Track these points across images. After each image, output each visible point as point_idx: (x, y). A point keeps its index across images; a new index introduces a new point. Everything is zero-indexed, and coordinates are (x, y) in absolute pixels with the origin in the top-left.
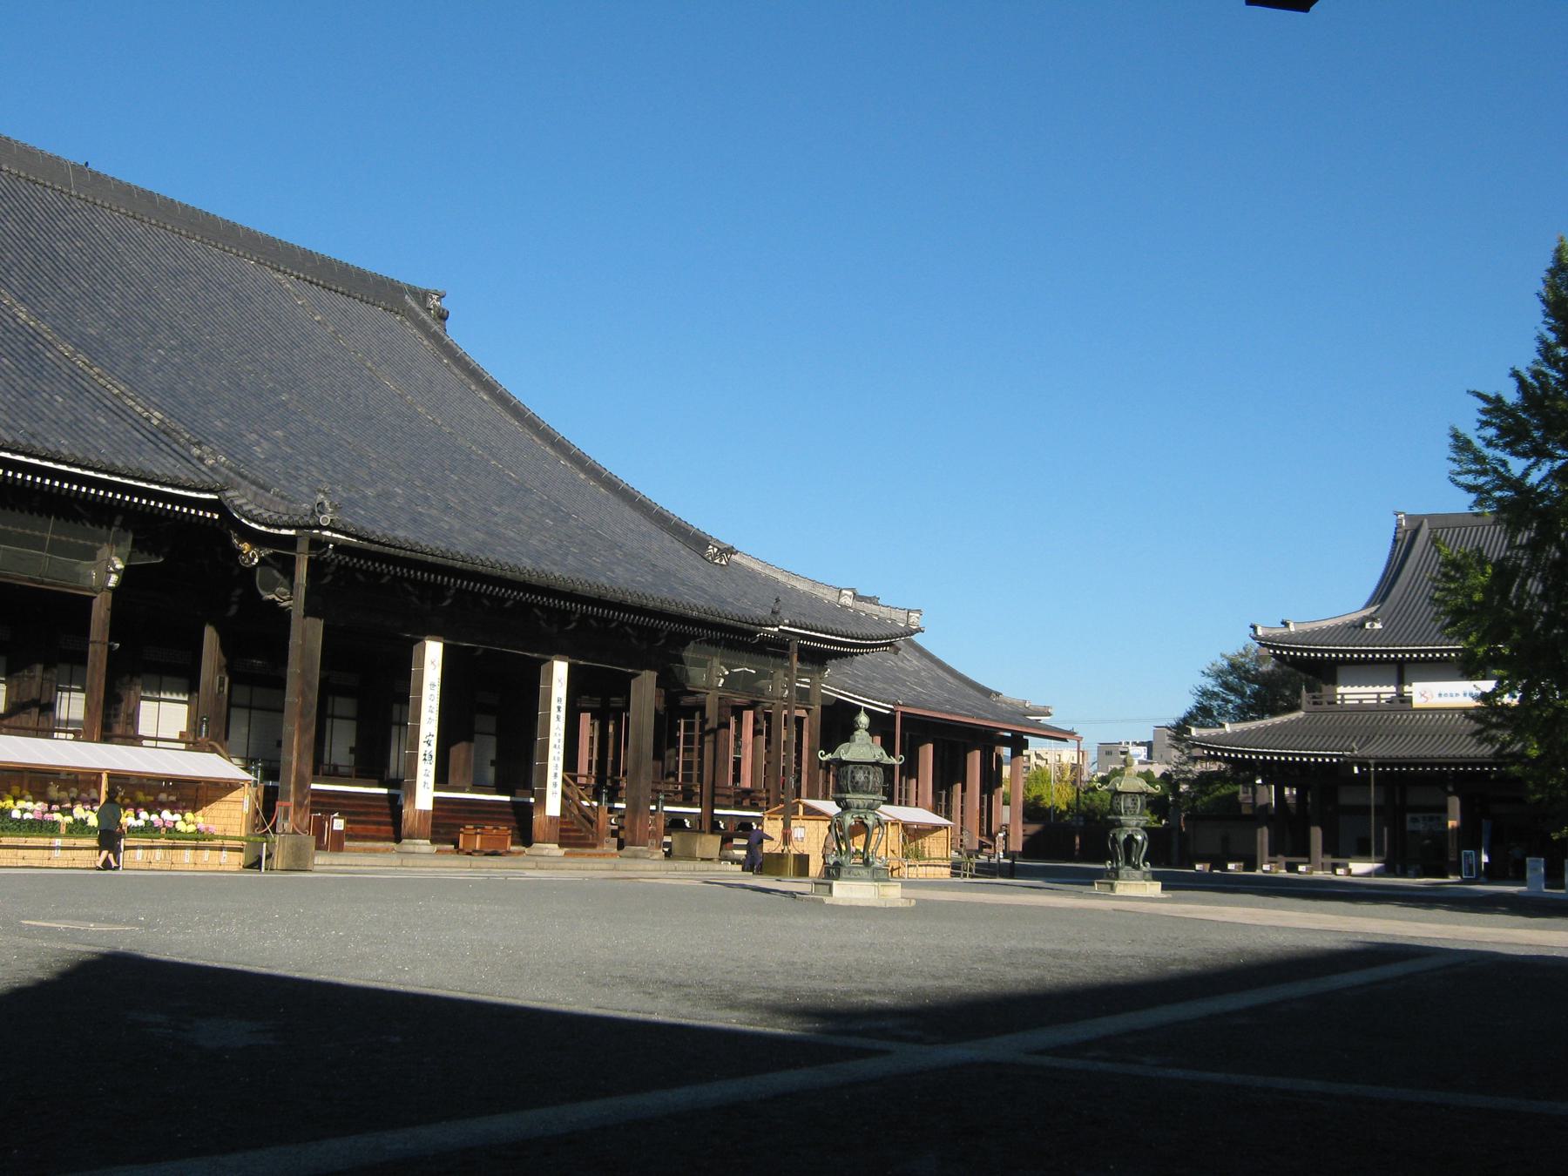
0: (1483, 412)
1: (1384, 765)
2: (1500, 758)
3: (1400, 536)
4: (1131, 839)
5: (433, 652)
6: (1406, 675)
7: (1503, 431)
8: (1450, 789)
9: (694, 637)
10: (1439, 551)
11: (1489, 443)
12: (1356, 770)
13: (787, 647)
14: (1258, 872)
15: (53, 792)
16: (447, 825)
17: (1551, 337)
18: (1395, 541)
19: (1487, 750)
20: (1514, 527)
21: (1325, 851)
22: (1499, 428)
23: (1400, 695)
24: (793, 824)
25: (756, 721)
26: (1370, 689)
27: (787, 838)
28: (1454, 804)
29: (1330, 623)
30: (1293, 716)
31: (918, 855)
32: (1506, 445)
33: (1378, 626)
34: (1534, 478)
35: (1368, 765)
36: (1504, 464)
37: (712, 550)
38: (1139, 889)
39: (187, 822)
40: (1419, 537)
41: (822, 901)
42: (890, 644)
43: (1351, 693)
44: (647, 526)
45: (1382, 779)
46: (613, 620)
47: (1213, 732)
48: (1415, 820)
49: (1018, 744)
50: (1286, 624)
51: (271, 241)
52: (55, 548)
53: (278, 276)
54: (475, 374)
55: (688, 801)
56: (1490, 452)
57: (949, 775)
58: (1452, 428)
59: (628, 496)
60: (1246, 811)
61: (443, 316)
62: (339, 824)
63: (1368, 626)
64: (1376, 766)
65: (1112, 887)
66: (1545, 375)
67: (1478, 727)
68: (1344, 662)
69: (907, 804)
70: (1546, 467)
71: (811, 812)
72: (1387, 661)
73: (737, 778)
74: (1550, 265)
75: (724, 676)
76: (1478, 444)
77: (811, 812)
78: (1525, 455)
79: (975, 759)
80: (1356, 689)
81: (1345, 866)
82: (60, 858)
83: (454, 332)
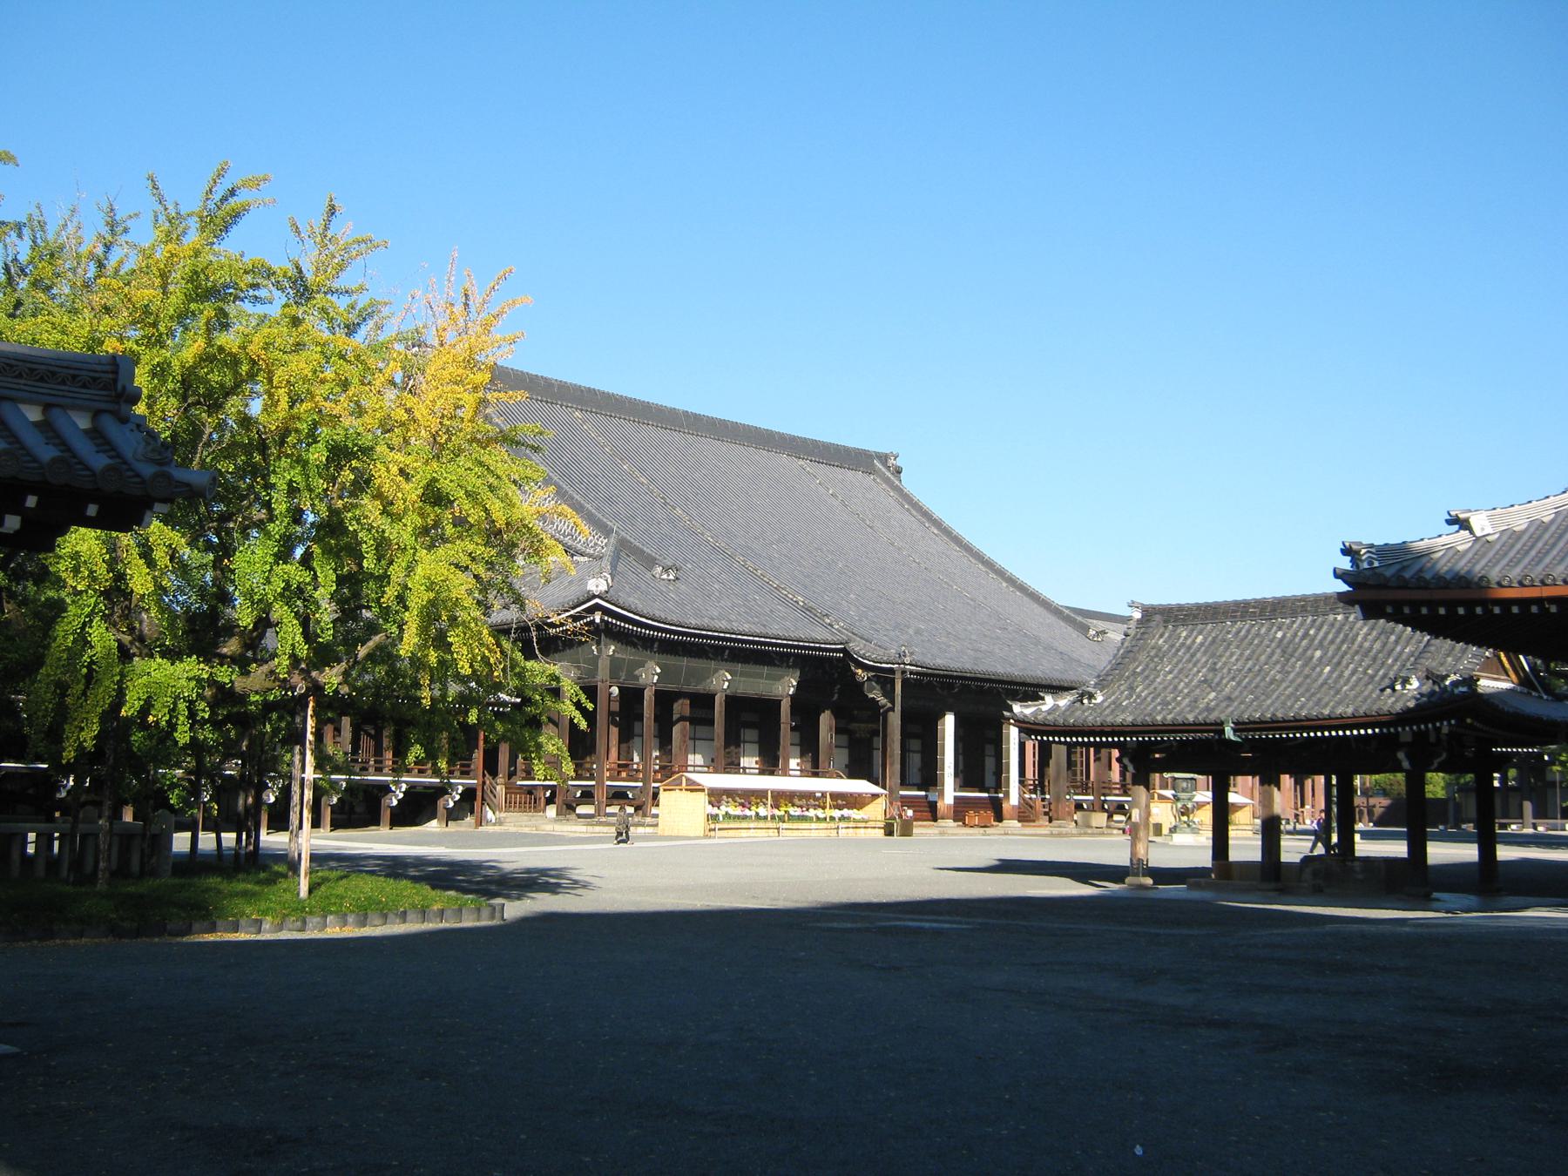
5: (949, 721)
15: (796, 801)
16: (961, 811)
37: (1092, 632)
39: (854, 814)
44: (1051, 619)
51: (793, 439)
52: (769, 677)
53: (801, 462)
54: (927, 515)
61: (898, 471)
62: (910, 813)
71: (1162, 797)
77: (1162, 797)
82: (814, 834)
83: (908, 482)
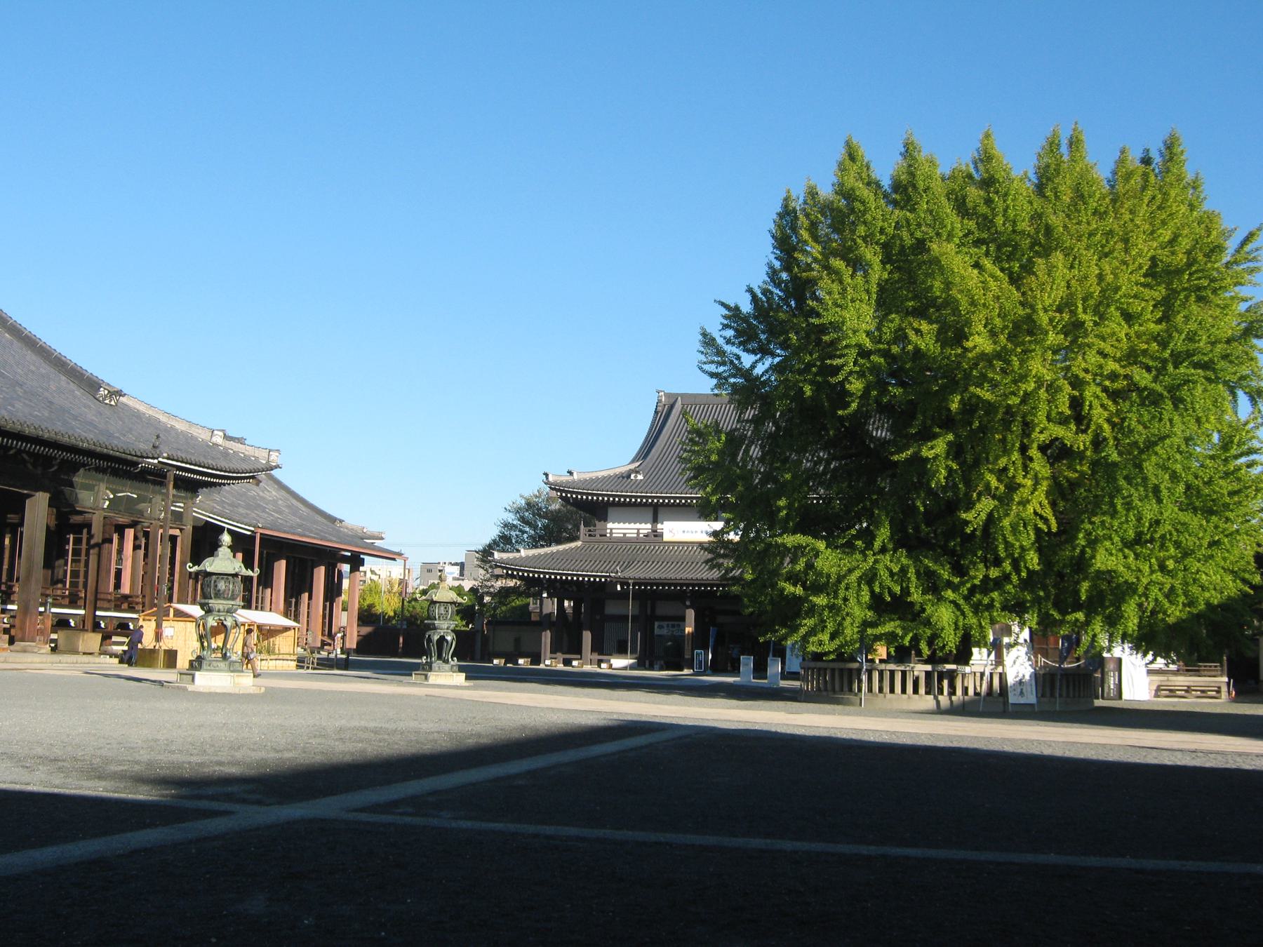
0: (725, 317)
1: (640, 584)
2: (725, 580)
3: (660, 409)
4: (442, 639)
7: (739, 333)
8: (688, 603)
9: (84, 465)
10: (687, 421)
11: (728, 342)
12: (619, 588)
13: (165, 477)
14: (542, 666)
17: (777, 264)
18: (656, 412)
19: (715, 574)
20: (742, 406)
21: (593, 650)
22: (736, 330)
23: (654, 531)
24: (165, 624)
25: (136, 538)
26: (632, 526)
27: (158, 636)
28: (690, 614)
29: (605, 474)
30: (573, 545)
31: (270, 651)
32: (741, 343)
33: (640, 477)
34: (759, 370)
35: (628, 585)
36: (738, 358)
37: (102, 392)
38: (447, 679)
40: (674, 411)
41: (185, 689)
42: (253, 477)
43: (619, 528)
44: (45, 369)
45: (637, 595)
46: (11, 448)
47: (511, 555)
48: (660, 627)
49: (356, 562)
50: (571, 473)
55: (73, 603)
56: (728, 348)
57: (298, 586)
58: (702, 328)
59: (31, 343)
60: (534, 618)
63: (632, 477)
64: (634, 585)
65: (426, 677)
66: (772, 293)
67: (710, 556)
68: (614, 504)
69: (262, 609)
70: (768, 362)
71: (180, 614)
72: (646, 505)
73: (118, 585)
74: (779, 210)
75: (109, 499)
76: (720, 341)
77: (180, 614)
78: (754, 352)
79: (320, 573)
80: (621, 525)
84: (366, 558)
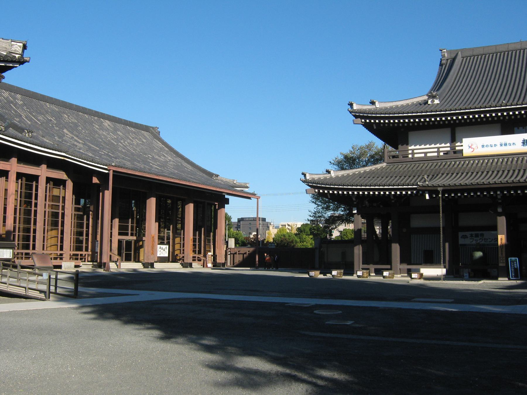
6: (457, 135)
8: (500, 210)
12: (427, 197)
18: (441, 65)
21: (402, 262)
23: (453, 148)
28: (502, 222)
30: (378, 166)
33: (437, 101)
35: (437, 192)
40: (457, 61)
43: (421, 150)
48: (465, 237)
50: (373, 103)
63: (429, 102)
64: (444, 192)
69: (119, 235)
81: (417, 271)
84: (231, 198)
